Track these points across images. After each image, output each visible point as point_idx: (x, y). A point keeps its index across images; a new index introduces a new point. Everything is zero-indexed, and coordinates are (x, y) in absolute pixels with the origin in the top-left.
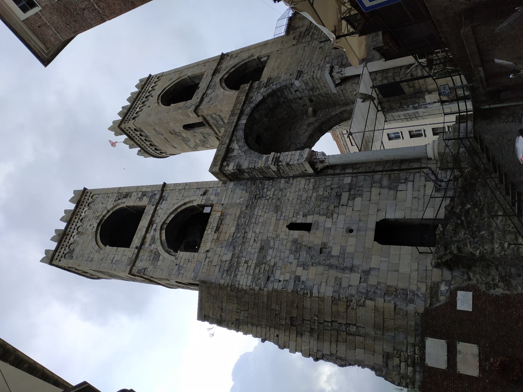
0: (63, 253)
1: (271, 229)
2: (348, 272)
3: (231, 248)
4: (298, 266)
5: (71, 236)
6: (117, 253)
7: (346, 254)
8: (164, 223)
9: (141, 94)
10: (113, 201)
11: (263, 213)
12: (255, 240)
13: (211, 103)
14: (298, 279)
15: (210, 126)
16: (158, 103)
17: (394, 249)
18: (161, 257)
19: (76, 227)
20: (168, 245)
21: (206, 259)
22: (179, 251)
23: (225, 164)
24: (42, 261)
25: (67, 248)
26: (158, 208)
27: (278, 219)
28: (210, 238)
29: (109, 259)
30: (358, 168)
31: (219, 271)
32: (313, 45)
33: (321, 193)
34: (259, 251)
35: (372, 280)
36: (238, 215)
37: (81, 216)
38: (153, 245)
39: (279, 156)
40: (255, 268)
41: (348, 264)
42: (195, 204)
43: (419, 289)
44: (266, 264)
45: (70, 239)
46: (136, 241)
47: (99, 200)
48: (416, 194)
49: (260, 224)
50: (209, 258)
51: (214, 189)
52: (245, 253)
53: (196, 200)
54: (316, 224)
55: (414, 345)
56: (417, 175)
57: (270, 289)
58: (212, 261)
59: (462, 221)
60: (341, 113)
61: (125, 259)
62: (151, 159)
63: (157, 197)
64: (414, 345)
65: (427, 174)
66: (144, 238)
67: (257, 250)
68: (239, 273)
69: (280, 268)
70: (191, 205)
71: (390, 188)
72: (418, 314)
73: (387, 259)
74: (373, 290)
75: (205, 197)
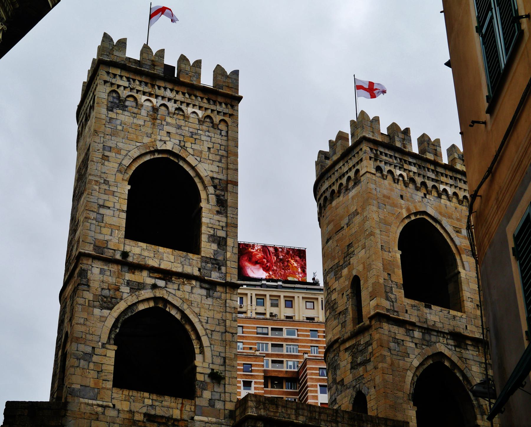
0: (119, 86)
5: (150, 95)
6: (117, 213)
8: (166, 302)
9: (432, 167)
10: (211, 174)
13: (392, 345)
15: (355, 335)
16: (408, 217)
18: (106, 312)
19: (166, 102)
21: (101, 406)
22: (116, 348)
24: (106, 37)
25: (127, 93)
26: (194, 282)
28: (137, 406)
29: (106, 197)
37: (188, 105)
42: (198, 360)
45: (144, 93)
46: (138, 250)
47: (218, 139)
50: (103, 413)
51: (223, 395)
53: (204, 361)
58: (97, 419)
61: (105, 235)
62: (314, 179)
63: (215, 276)
70: (197, 351)
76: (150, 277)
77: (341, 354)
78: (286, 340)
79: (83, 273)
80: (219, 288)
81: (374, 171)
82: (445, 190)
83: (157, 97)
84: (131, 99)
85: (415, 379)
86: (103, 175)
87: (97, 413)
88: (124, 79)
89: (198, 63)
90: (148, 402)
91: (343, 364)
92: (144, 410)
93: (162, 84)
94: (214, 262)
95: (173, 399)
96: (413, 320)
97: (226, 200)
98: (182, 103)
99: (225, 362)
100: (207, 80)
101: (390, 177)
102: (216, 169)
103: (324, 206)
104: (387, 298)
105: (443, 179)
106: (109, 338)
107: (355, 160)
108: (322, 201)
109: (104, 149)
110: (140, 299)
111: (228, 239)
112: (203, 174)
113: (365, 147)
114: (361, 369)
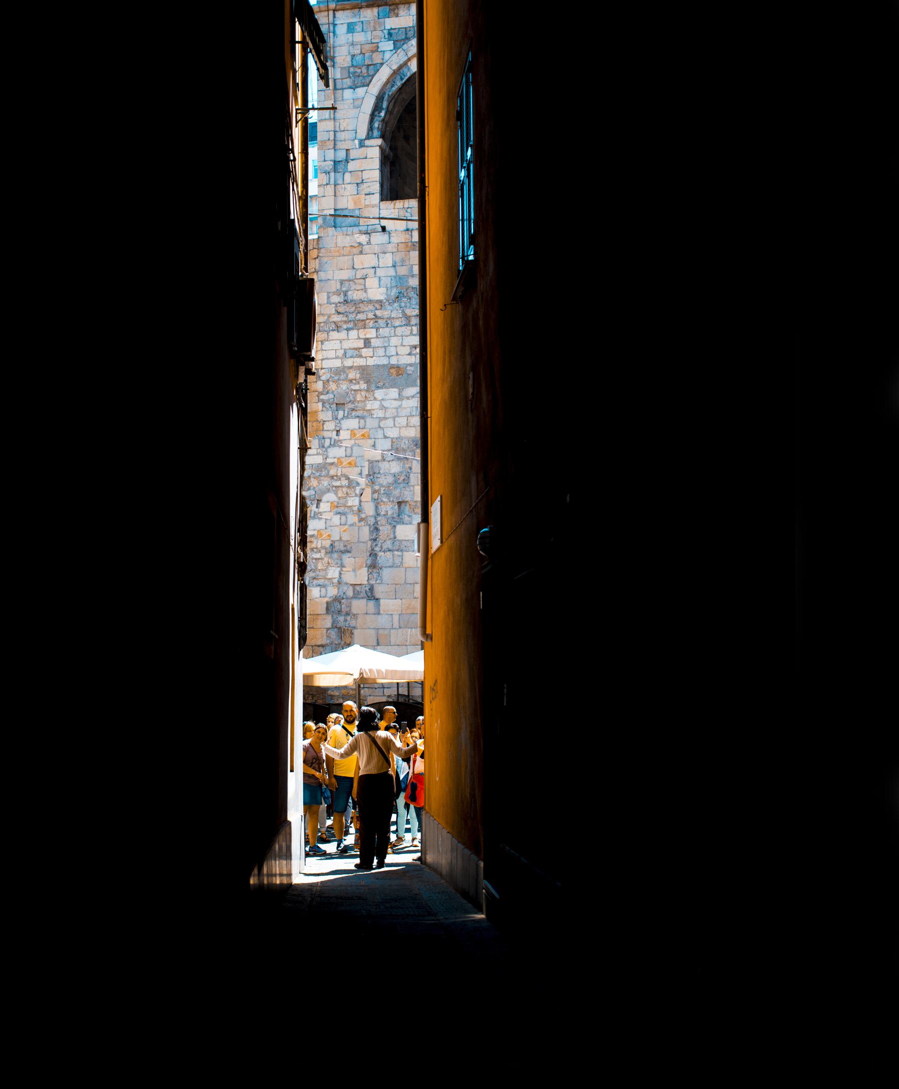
2: (369, 562)
7: (399, 553)
18: (361, 91)
20: (403, 85)
31: (342, 282)
34: (392, 367)
35: (359, 606)
38: (389, 45)
41: (384, 558)
44: (367, 391)
50: (369, 243)
52: (384, 332)
57: (322, 416)
58: (361, 253)
67: (394, 361)
68: (343, 334)
73: (396, 625)
87: (360, 244)
106: (371, 128)
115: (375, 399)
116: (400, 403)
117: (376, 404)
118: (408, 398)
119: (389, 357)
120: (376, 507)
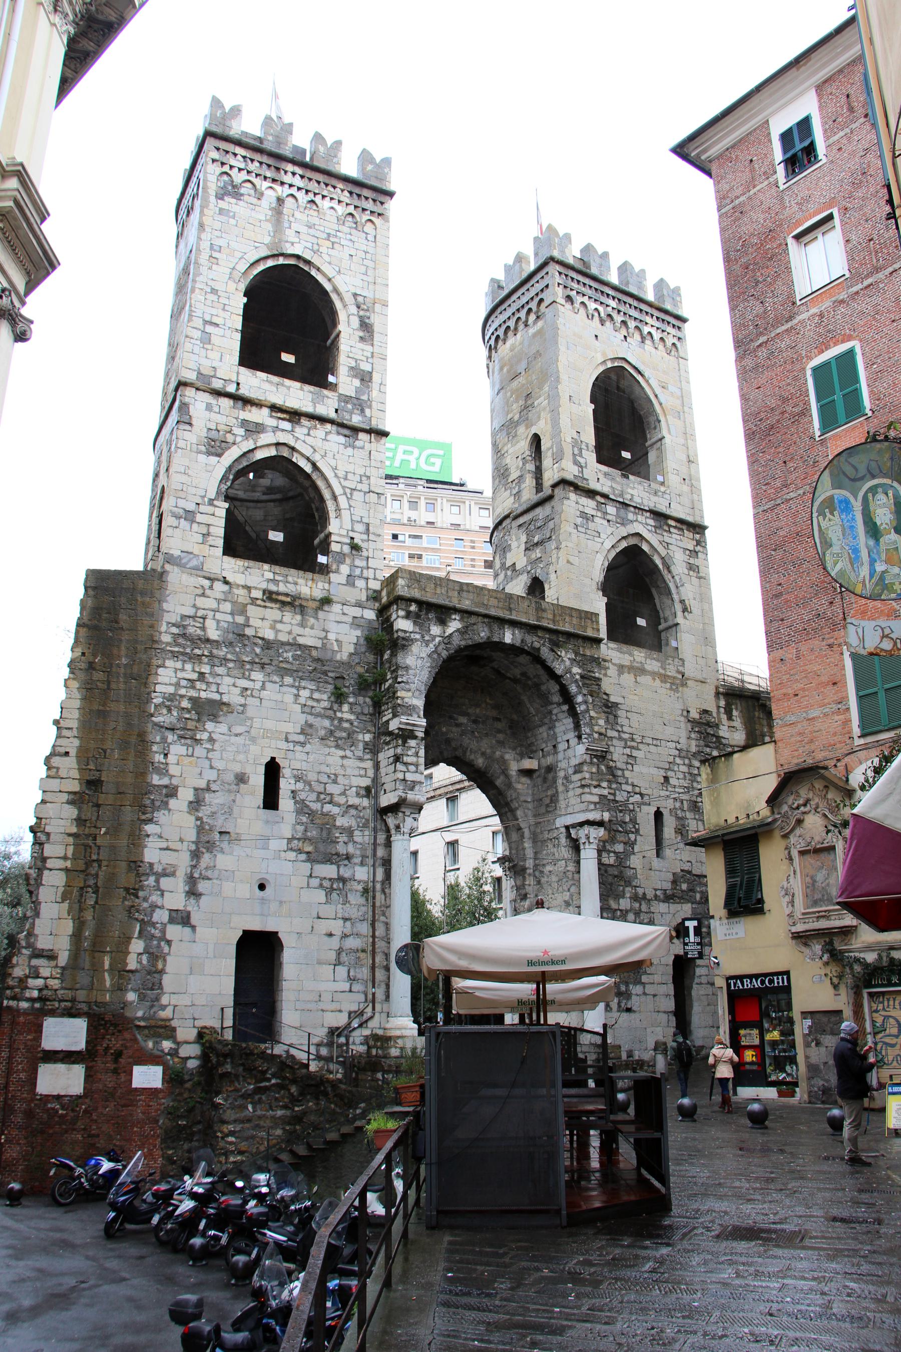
0: (231, 167)
1: (270, 724)
2: (187, 888)
3: (231, 635)
4: (196, 789)
5: (274, 181)
8: (293, 449)
9: (635, 303)
11: (302, 700)
12: (247, 689)
14: (172, 792)
17: (230, 964)
22: (227, 505)
23: (413, 608)
24: (216, 103)
27: (291, 738)
30: (383, 891)
31: (184, 617)
32: (678, 760)
33: (338, 823)
35: (174, 932)
36: (301, 641)
37: (324, 197)
38: (241, 431)
39: (415, 737)
40: (191, 699)
41: (202, 886)
42: (334, 526)
43: (164, 1008)
45: (265, 178)
46: (256, 383)
48: (326, 997)
49: (278, 697)
50: (211, 588)
51: (365, 571)
52: (220, 670)
54: (277, 819)
55: (73, 1000)
56: (362, 997)
57: (150, 737)
59: (269, 1080)
60: (520, 829)
63: (356, 420)
64: (73, 1000)
65: (362, 1013)
66: (258, 404)
68: (179, 665)
69: (190, 753)
70: (332, 515)
71: (339, 952)
72: (123, 1008)
73: (211, 955)
74: (157, 933)
75: (346, 549)
76: (271, 416)
77: (514, 531)
78: (426, 549)
79: (184, 407)
80: (362, 435)
81: (563, 301)
82: (650, 333)
83: (282, 183)
84: (249, 185)
85: (606, 564)
86: (210, 283)
88: (239, 157)
89: (338, 143)
90: (270, 576)
91: (514, 544)
92: (264, 585)
93: (290, 167)
94: (355, 401)
95: (301, 573)
96: (606, 490)
97: (372, 326)
98: (315, 194)
99: (368, 529)
100: (349, 167)
101: (582, 310)
102: (360, 283)
103: (496, 348)
104: (576, 463)
105: (648, 319)
107: (538, 287)
108: (492, 342)
109: (212, 248)
110: (259, 444)
111: (374, 374)
112: (342, 288)
113: (553, 268)
114: (537, 553)
115: (205, 730)
116: (227, 738)
117: (205, 736)
118: (236, 735)
119: (221, 694)
120: (198, 833)
